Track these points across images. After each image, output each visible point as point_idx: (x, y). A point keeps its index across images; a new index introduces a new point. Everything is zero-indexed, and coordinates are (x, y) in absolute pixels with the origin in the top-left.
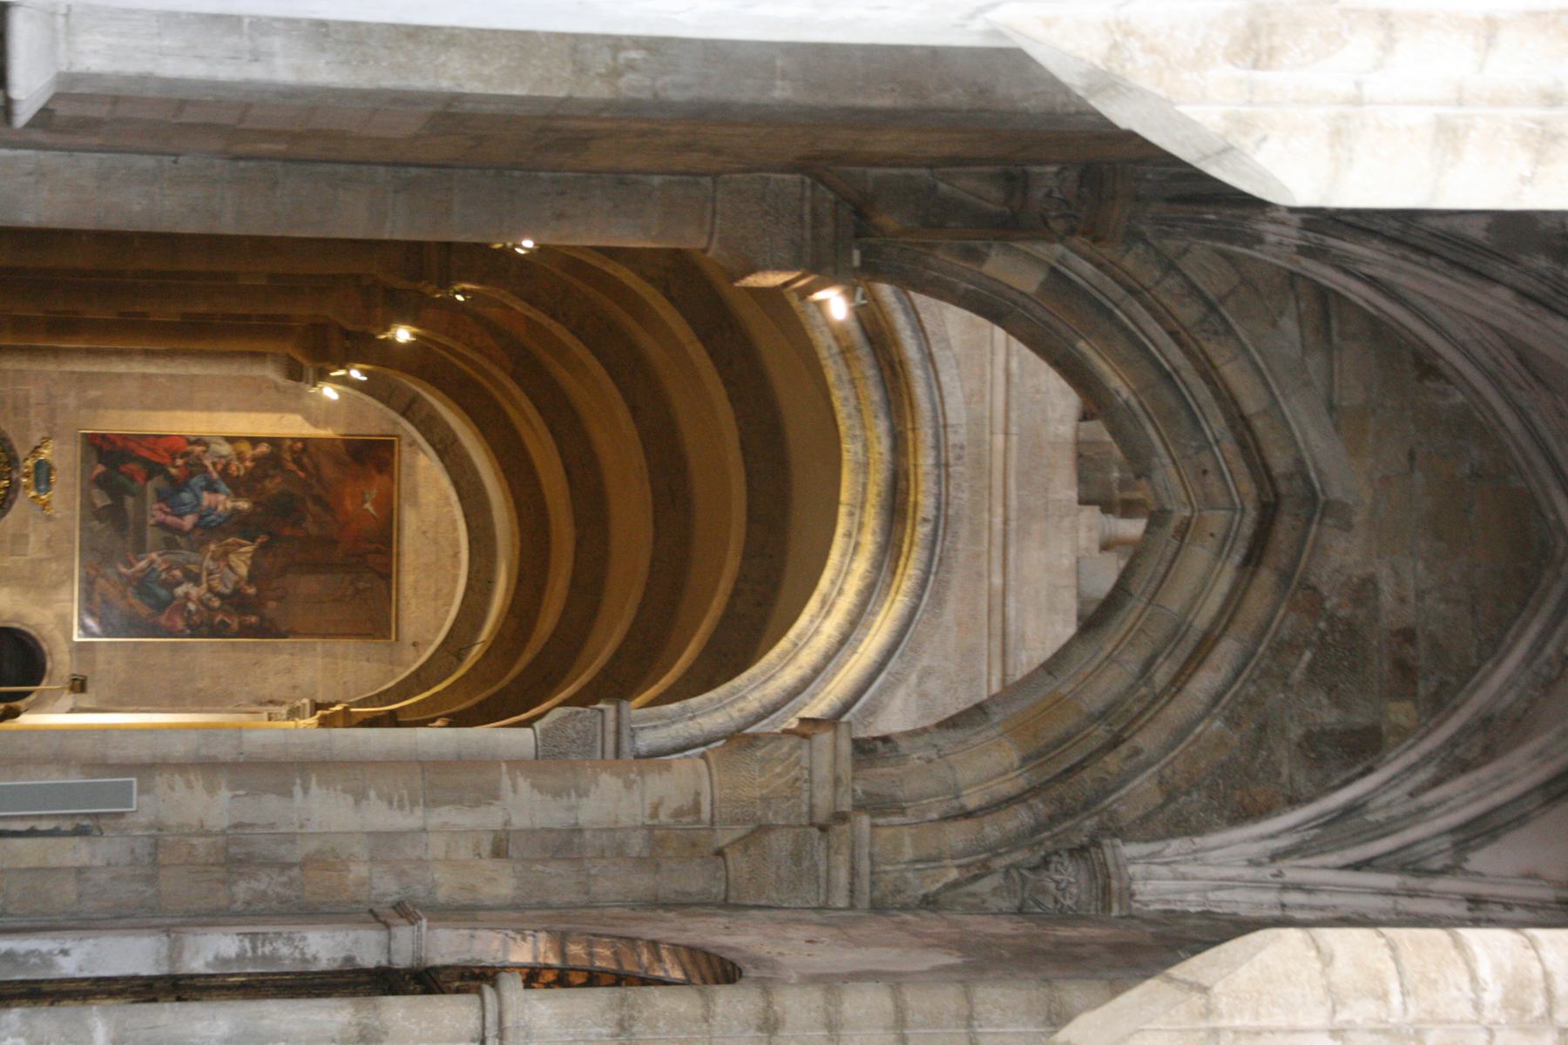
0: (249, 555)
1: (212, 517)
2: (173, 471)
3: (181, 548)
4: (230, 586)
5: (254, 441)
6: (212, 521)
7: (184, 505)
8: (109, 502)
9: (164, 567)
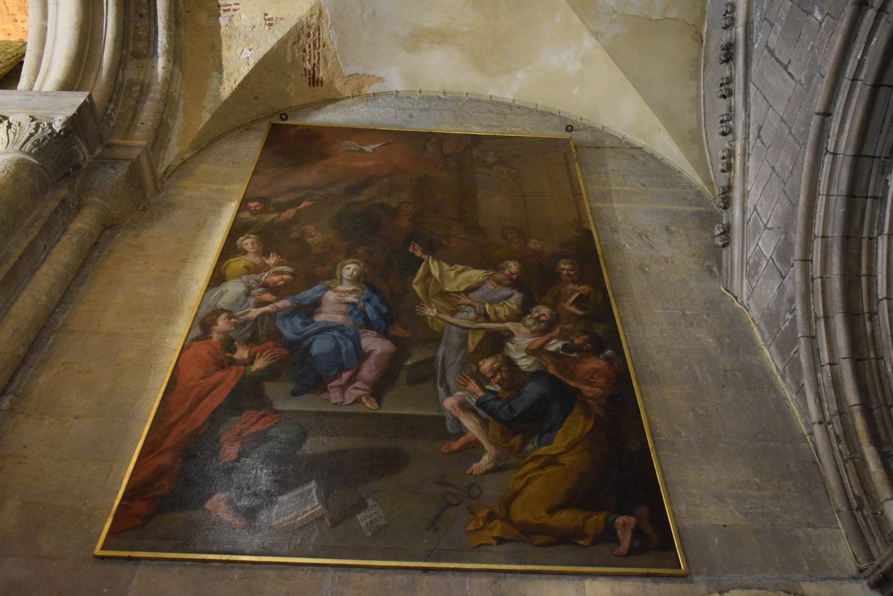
0: (446, 267)
1: (369, 309)
2: (260, 364)
3: (433, 359)
4: (506, 292)
5: (230, 250)
6: (377, 309)
7: (338, 348)
8: (313, 485)
9: (473, 386)
